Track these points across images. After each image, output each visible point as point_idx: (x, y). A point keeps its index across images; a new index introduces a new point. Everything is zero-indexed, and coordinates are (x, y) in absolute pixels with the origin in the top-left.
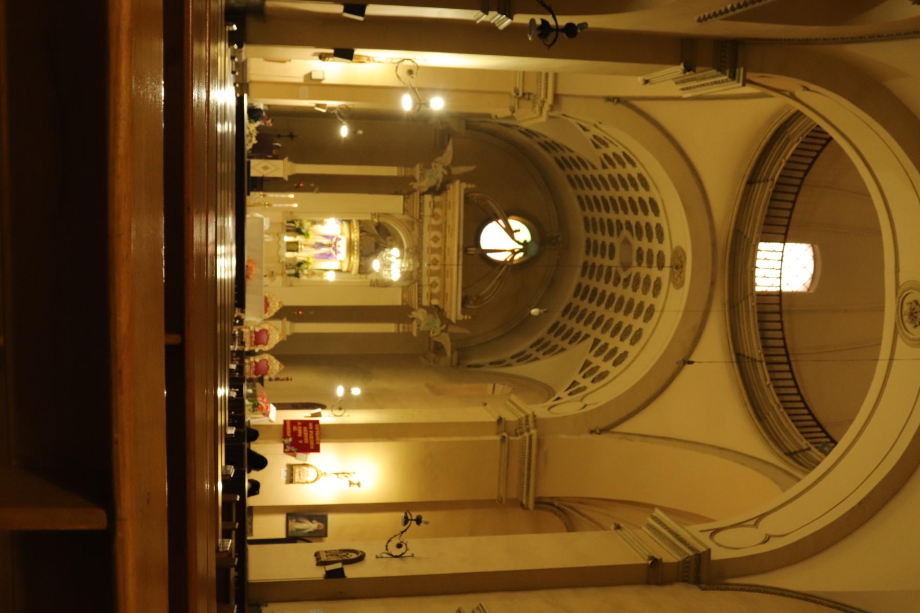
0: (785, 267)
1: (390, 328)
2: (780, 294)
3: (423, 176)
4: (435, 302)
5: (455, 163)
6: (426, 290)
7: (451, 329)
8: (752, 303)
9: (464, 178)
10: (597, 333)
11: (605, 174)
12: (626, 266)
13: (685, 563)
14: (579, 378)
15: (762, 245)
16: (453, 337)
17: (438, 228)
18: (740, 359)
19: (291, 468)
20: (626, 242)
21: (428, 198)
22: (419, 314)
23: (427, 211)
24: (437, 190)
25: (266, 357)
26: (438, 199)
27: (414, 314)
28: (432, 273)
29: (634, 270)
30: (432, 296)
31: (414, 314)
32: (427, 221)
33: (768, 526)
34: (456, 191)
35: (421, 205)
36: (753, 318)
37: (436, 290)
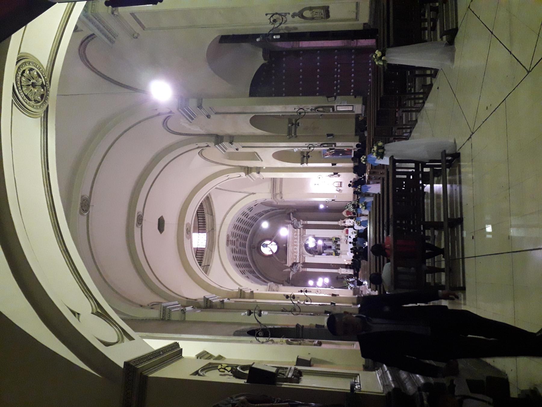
0: (199, 240)
1: (309, 222)
2: (199, 232)
3: (299, 268)
4: (296, 230)
5: (289, 272)
6: (298, 234)
7: (291, 222)
8: (207, 230)
9: (287, 267)
10: (246, 219)
11: (244, 269)
12: (237, 240)
13: (251, 172)
14: (254, 207)
15: (204, 247)
16: (290, 219)
17: (295, 252)
18: (212, 214)
19: (341, 186)
20: (237, 247)
21: (298, 262)
22: (300, 226)
23: (298, 257)
24: (295, 264)
25: (347, 216)
26: (295, 261)
27: (302, 226)
28: (297, 239)
29: (235, 239)
30: (297, 232)
31: (302, 226)
32: (298, 255)
33: (227, 178)
34: (289, 264)
35: (300, 259)
36: (207, 226)
37: (295, 233)
